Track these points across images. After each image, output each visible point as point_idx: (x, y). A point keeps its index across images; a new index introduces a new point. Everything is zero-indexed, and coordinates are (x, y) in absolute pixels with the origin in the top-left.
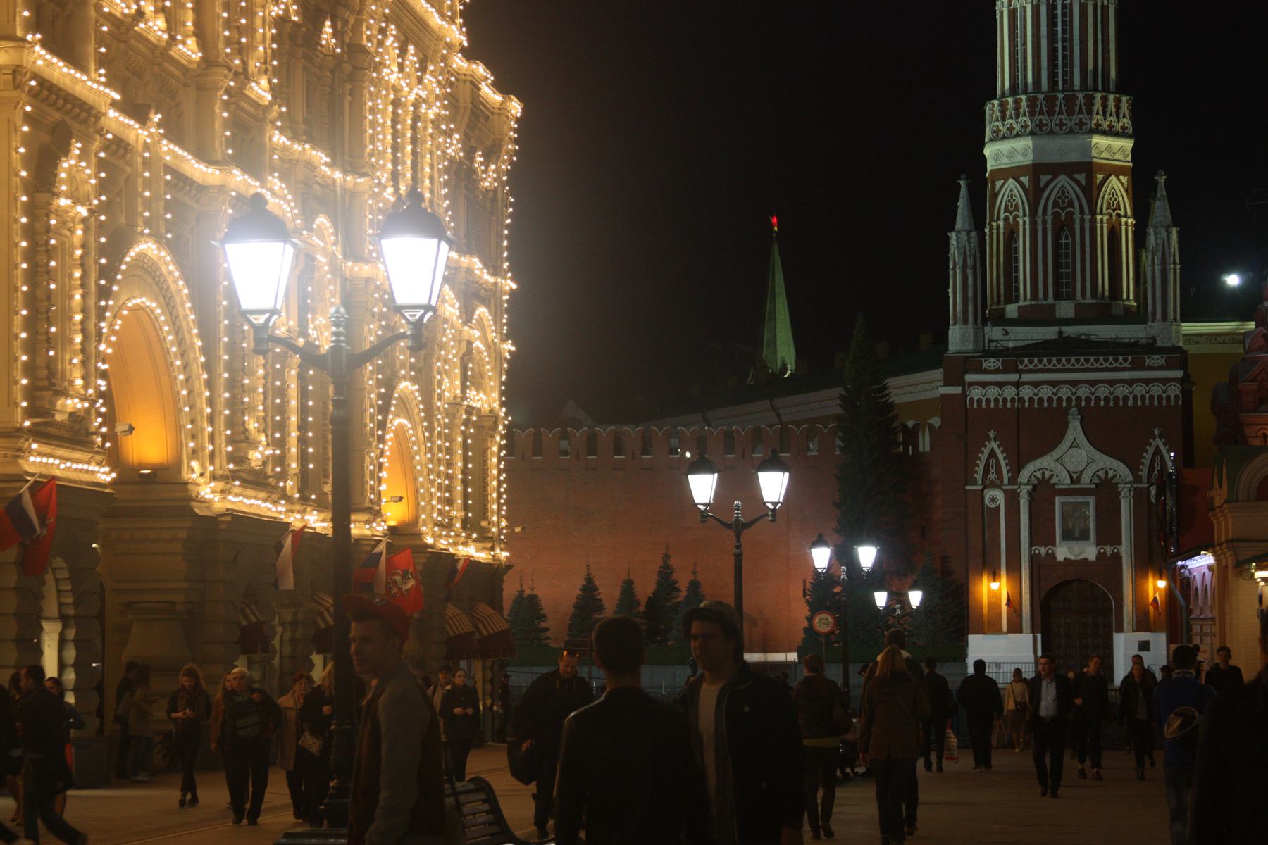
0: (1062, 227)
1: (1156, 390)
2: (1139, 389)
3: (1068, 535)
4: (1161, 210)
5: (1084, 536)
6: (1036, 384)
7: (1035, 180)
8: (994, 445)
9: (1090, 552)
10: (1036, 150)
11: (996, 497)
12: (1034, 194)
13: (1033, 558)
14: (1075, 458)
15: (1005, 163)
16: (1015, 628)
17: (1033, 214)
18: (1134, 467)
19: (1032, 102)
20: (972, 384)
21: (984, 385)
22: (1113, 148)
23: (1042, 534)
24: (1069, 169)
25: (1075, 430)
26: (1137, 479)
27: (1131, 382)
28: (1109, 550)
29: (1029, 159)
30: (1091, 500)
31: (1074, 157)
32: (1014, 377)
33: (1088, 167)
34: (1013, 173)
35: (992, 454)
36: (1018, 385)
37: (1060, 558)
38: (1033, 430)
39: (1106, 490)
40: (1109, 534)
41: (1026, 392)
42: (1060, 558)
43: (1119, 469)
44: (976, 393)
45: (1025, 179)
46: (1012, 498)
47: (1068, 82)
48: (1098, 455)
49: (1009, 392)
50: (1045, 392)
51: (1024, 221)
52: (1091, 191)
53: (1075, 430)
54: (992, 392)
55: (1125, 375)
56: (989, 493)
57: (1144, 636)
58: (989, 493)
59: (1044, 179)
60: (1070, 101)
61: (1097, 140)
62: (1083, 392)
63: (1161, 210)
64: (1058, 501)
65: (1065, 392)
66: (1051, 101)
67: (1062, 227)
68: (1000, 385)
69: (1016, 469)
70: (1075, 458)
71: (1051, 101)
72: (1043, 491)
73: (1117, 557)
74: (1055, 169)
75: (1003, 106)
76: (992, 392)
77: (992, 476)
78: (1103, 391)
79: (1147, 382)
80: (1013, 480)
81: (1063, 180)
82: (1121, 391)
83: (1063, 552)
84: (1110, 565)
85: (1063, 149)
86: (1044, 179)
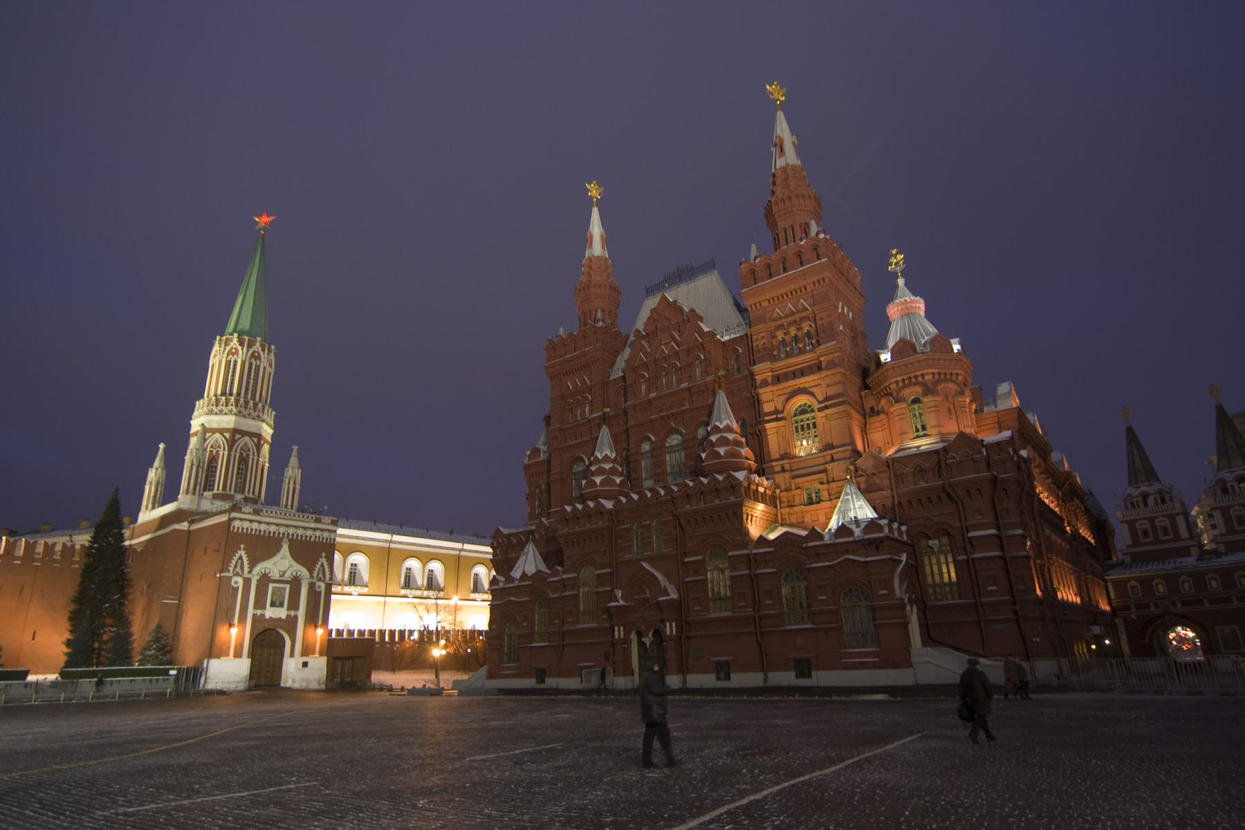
0: (244, 460)
1: (326, 534)
2: (318, 533)
3: (273, 604)
4: (294, 461)
5: (281, 605)
6: (268, 524)
7: (233, 436)
8: (242, 553)
9: (282, 613)
10: (236, 422)
11: (238, 582)
12: (232, 443)
13: (254, 615)
14: (282, 564)
15: (215, 426)
16: (238, 654)
17: (230, 450)
18: (311, 571)
19: (237, 401)
20: (235, 519)
21: (241, 520)
22: (267, 431)
23: (260, 604)
24: (251, 435)
25: (285, 549)
26: (312, 577)
27: (314, 529)
28: (292, 613)
29: (232, 426)
30: (288, 587)
31: (254, 430)
32: (258, 518)
33: (259, 436)
34: (221, 431)
35: (241, 558)
36: (259, 522)
37: (267, 617)
38: (264, 547)
39: (295, 582)
40: (294, 605)
41: (263, 527)
42: (267, 617)
43: (303, 572)
44: (237, 524)
45: (227, 435)
46: (247, 582)
47: (253, 398)
48: (294, 563)
49: (255, 526)
50: (272, 528)
51: (223, 454)
52: (259, 447)
53: (285, 549)
54: (246, 525)
55: (313, 525)
56: (234, 579)
57: (305, 659)
58: (234, 579)
59: (238, 436)
60: (255, 405)
61: (264, 426)
62: (291, 531)
63: (294, 461)
64: (271, 586)
65: (282, 530)
66: (246, 403)
67: (244, 460)
68: (251, 521)
69: (252, 566)
70: (282, 564)
71: (246, 403)
72: (265, 580)
73: (296, 617)
74: (244, 433)
75: (217, 401)
76: (246, 525)
77: (238, 569)
78: (300, 532)
79: (322, 530)
80: (250, 572)
81: (247, 439)
82: (309, 533)
83: (270, 613)
84: (291, 624)
85: (249, 425)
86: (238, 436)
